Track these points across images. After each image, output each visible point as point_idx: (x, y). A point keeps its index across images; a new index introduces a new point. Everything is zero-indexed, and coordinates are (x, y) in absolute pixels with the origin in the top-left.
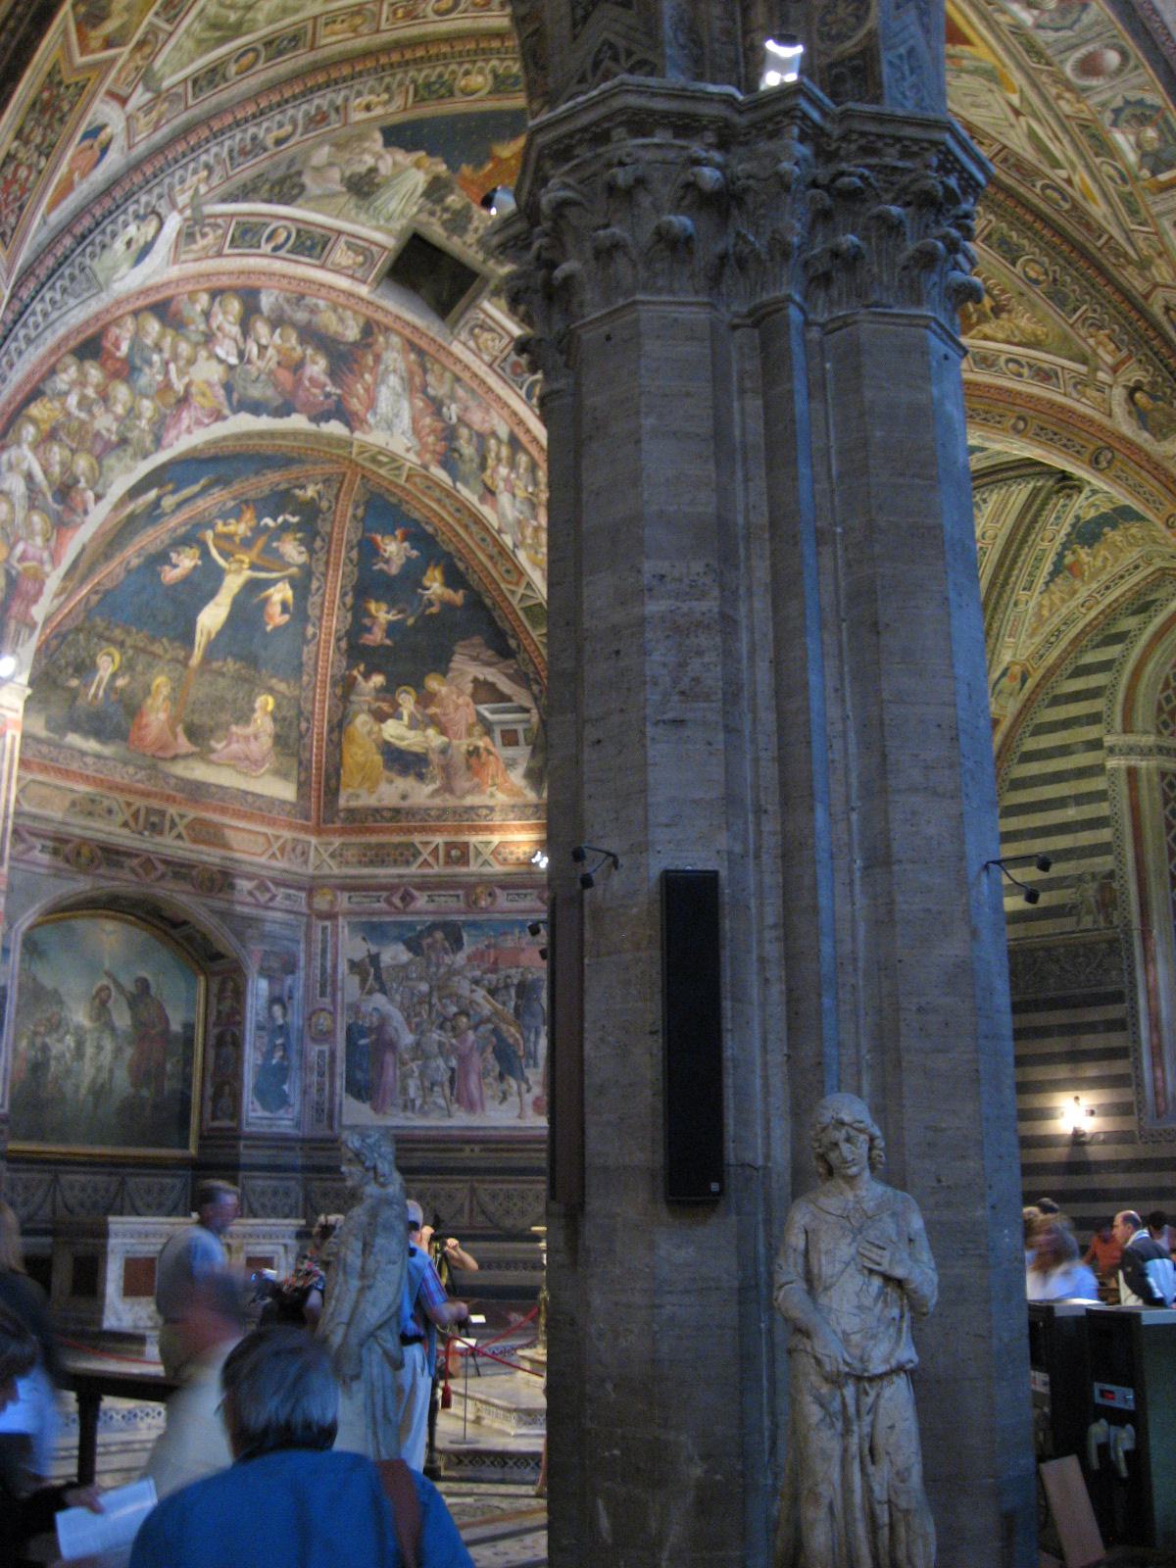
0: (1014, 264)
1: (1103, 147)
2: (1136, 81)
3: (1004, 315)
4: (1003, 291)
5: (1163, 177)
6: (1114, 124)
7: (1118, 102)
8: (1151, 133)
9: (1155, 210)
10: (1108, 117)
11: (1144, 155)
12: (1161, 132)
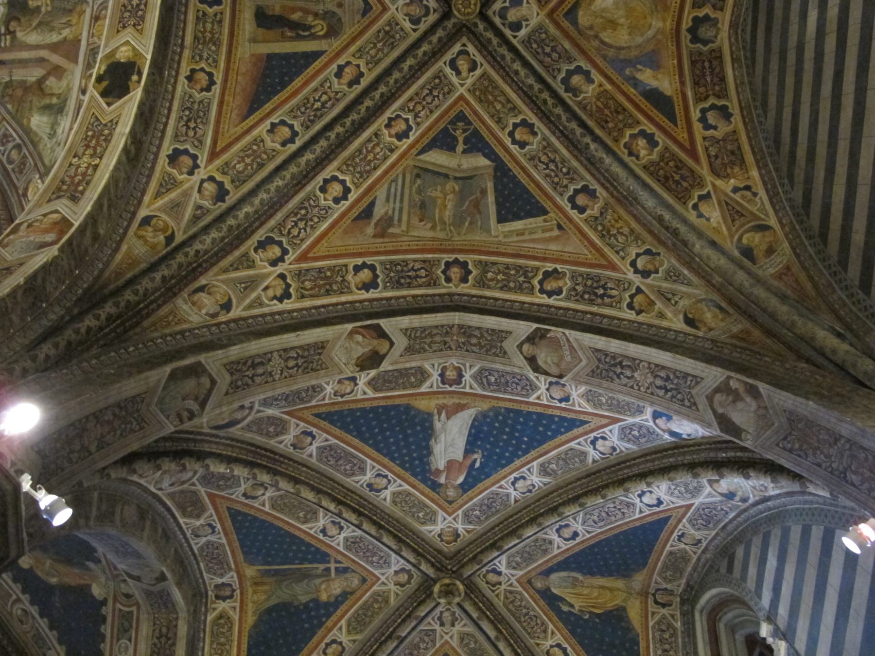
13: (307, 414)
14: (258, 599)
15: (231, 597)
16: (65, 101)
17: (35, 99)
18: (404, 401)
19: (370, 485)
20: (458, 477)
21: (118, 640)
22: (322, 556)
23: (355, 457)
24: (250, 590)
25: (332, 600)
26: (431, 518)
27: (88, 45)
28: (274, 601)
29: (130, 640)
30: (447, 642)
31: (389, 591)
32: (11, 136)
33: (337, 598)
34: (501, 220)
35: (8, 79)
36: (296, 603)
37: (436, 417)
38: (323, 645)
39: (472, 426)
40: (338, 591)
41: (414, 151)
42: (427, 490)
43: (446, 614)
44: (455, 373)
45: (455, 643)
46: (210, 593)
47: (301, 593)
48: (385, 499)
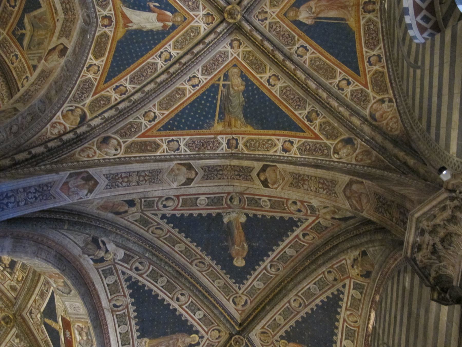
13: (102, 86)
14: (240, 125)
15: (237, 140)
18: (115, 43)
19: (166, 61)
20: (167, 15)
21: (262, 207)
22: (214, 88)
23: (143, 67)
24: (234, 129)
25: (244, 83)
26: (196, 30)
28: (241, 116)
29: (260, 199)
30: (277, 15)
31: (243, 51)
33: (243, 80)
34: (40, 7)
36: (244, 103)
37: (130, 28)
38: (269, 87)
39: (133, 8)
40: (240, 80)
41: (22, 51)
42: (175, 31)
43: (260, 17)
44: (105, 20)
45: (277, 10)
46: (233, 152)
47: (238, 101)
48: (178, 53)
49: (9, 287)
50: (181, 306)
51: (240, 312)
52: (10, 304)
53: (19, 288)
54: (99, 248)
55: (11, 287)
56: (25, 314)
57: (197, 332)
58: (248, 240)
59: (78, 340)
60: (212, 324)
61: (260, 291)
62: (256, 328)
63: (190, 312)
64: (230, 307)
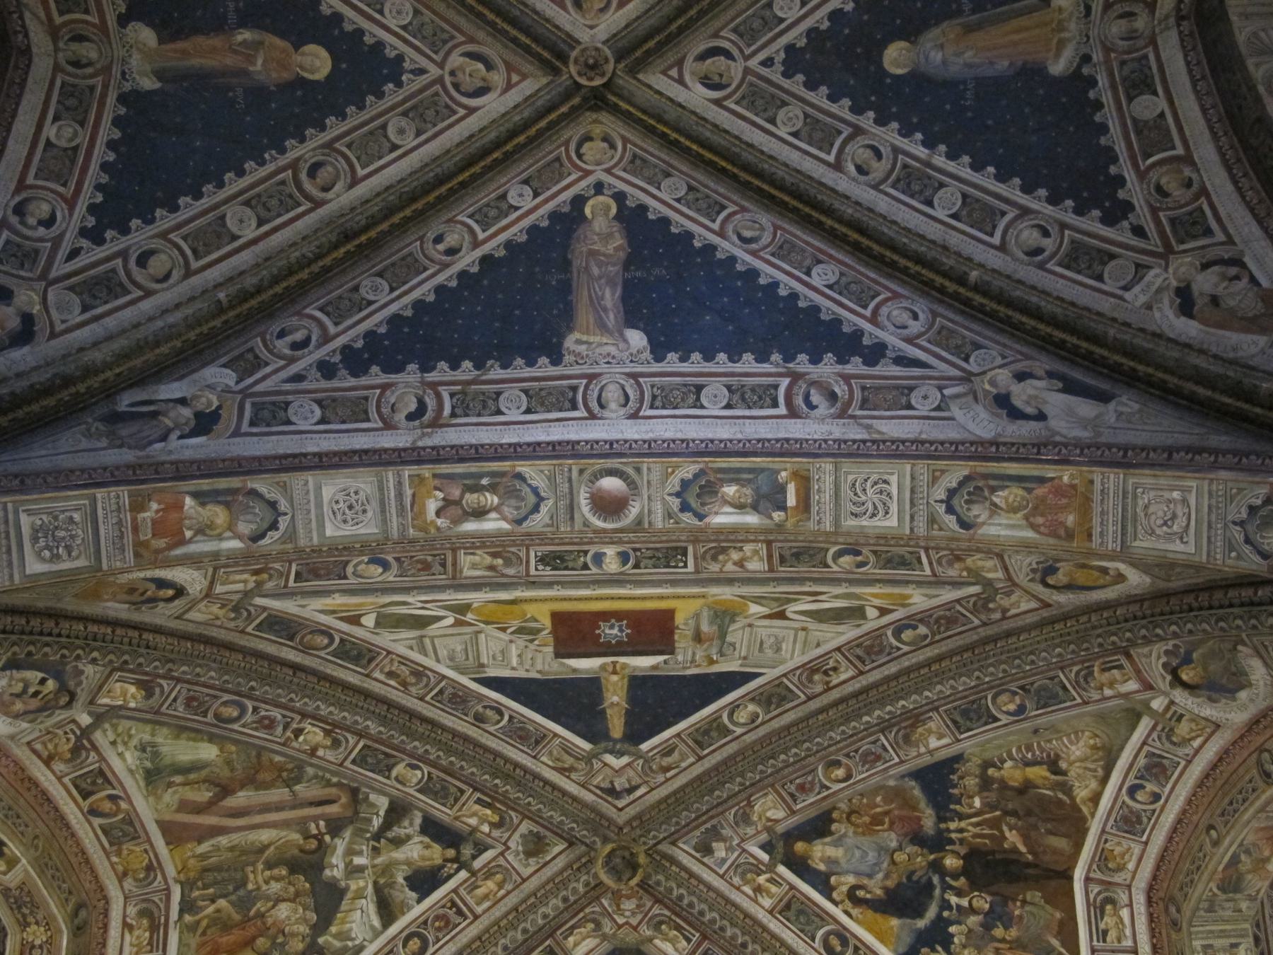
0: (996, 719)
1: (729, 538)
2: (655, 477)
3: (1063, 765)
4: (1029, 748)
5: (791, 501)
6: (701, 517)
7: (675, 503)
8: (730, 490)
9: (828, 526)
10: (687, 518)
11: (755, 507)
12: (736, 481)
16: (147, 785)
17: (226, 773)
27: (149, 840)
32: (256, 729)
35: (297, 788)
49: (532, 861)
50: (476, 244)
51: (515, 78)
52: (584, 860)
53: (525, 827)
54: (154, 415)
55: (529, 854)
56: (621, 812)
57: (579, 201)
58: (219, 26)
59: (505, 525)
60: (558, 159)
61: (421, 8)
62: (568, 28)
63: (504, 222)
64: (493, 106)
